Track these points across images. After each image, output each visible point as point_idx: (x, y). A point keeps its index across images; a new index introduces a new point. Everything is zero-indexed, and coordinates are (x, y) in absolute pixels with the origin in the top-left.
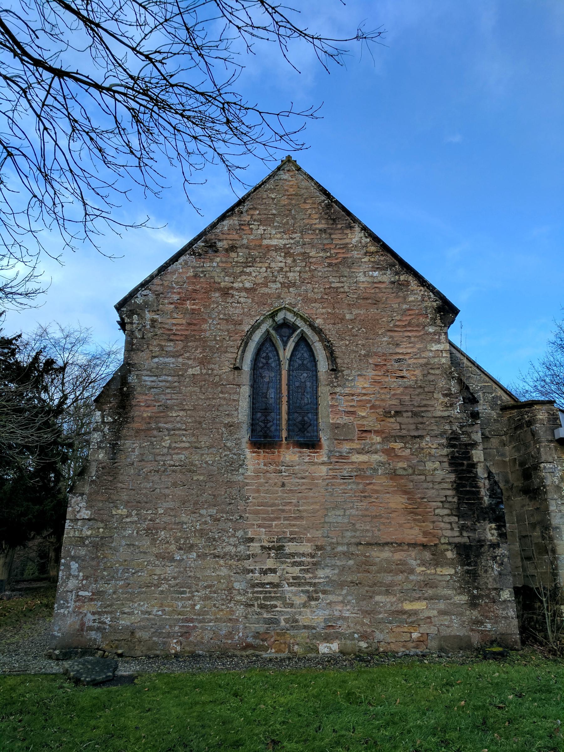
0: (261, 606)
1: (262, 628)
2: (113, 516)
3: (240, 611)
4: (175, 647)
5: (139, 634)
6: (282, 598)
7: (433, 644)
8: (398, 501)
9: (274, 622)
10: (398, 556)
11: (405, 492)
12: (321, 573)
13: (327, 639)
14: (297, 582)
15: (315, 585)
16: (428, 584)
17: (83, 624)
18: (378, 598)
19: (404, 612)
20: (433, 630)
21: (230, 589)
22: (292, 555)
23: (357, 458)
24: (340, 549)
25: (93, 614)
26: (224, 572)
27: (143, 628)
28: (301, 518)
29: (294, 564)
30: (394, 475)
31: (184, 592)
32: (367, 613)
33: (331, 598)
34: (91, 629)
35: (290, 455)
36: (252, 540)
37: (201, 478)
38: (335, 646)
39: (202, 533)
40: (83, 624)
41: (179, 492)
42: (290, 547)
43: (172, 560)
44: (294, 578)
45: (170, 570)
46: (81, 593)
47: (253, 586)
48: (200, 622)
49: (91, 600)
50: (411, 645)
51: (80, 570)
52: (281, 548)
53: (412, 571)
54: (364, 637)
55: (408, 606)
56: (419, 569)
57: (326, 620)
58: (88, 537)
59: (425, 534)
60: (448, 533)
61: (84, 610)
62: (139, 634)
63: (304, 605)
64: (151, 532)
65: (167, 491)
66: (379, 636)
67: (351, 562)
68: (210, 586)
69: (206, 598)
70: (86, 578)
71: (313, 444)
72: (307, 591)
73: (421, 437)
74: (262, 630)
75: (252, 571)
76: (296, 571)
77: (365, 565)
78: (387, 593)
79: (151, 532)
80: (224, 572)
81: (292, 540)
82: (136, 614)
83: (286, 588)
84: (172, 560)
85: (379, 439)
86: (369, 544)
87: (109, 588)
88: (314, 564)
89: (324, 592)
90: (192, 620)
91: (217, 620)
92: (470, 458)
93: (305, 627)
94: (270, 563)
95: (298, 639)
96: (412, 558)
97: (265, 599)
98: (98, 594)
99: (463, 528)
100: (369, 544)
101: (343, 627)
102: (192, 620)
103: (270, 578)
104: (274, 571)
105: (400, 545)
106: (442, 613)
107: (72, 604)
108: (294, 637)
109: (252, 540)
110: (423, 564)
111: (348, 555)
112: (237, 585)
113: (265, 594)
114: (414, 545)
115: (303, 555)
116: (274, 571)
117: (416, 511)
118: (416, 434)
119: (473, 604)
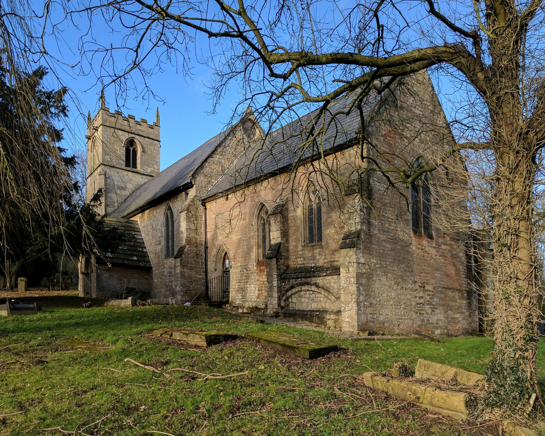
1: (419, 323)
3: (414, 315)
6: (425, 310)
9: (423, 321)
10: (453, 294)
12: (435, 299)
13: (437, 329)
14: (429, 303)
15: (433, 305)
16: (460, 307)
17: (367, 319)
18: (449, 312)
19: (454, 318)
20: (461, 326)
22: (428, 290)
23: (444, 247)
24: (440, 289)
25: (370, 314)
28: (428, 273)
29: (429, 295)
31: (397, 305)
32: (447, 318)
33: (438, 311)
35: (425, 242)
36: (416, 282)
37: (399, 247)
40: (367, 319)
42: (428, 287)
44: (428, 301)
46: (365, 303)
47: (417, 304)
50: (456, 332)
51: (364, 290)
52: (424, 287)
53: (456, 302)
54: (446, 328)
56: (459, 300)
57: (437, 321)
58: (365, 273)
59: (460, 285)
60: (465, 286)
65: (389, 252)
66: (449, 328)
67: (442, 296)
70: (366, 295)
71: (431, 237)
72: (431, 308)
73: (458, 240)
74: (420, 324)
75: (416, 297)
77: (446, 296)
78: (451, 310)
80: (409, 297)
81: (427, 283)
86: (447, 288)
89: (436, 309)
90: (401, 319)
94: (421, 294)
95: (430, 329)
96: (457, 295)
97: (422, 310)
101: (441, 324)
102: (401, 319)
103: (422, 301)
105: (454, 289)
106: (464, 319)
108: (429, 327)
109: (416, 282)
110: (459, 299)
111: (441, 292)
114: (457, 290)
115: (430, 291)
118: (457, 238)
119: (470, 316)
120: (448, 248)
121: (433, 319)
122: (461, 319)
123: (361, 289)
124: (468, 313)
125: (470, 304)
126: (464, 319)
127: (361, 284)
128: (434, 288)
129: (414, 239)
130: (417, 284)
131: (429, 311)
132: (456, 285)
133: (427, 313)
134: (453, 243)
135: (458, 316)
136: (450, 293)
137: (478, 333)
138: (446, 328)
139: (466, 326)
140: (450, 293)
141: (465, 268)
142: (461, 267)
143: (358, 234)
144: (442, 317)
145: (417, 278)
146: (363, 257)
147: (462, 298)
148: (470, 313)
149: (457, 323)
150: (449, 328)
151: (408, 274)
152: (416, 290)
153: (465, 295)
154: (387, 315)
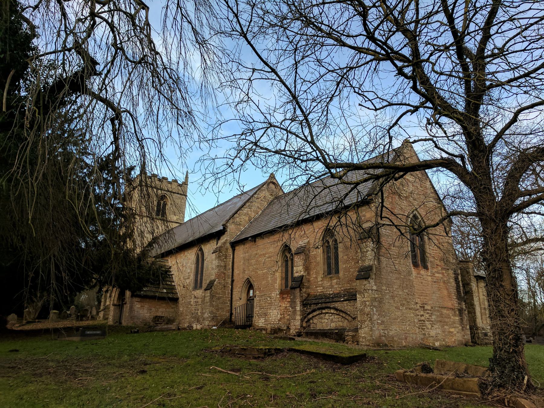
0: (422, 329)
1: (422, 336)
2: (382, 289)
4: (404, 344)
5: (395, 338)
6: (426, 326)
7: (457, 343)
8: (445, 292)
9: (424, 334)
10: (448, 312)
11: (447, 289)
12: (434, 317)
14: (429, 320)
15: (432, 321)
17: (380, 334)
18: (445, 327)
19: (450, 332)
21: (414, 322)
22: (427, 310)
23: (437, 275)
24: (437, 308)
26: (412, 315)
27: (395, 336)
28: (427, 296)
29: (428, 313)
30: (444, 282)
32: (444, 332)
33: (436, 326)
34: (383, 336)
35: (423, 272)
36: (417, 303)
38: (438, 343)
39: (405, 299)
40: (380, 334)
41: (398, 282)
42: (426, 307)
43: (400, 310)
45: (399, 314)
48: (409, 334)
49: (381, 324)
51: (377, 311)
52: (424, 307)
55: (452, 330)
56: (452, 317)
59: (452, 305)
60: (457, 305)
61: (380, 328)
62: (395, 339)
63: (431, 329)
64: (393, 297)
65: (395, 281)
68: (409, 320)
69: (409, 325)
70: (379, 315)
71: (426, 267)
76: (427, 315)
77: (442, 314)
78: (447, 325)
79: (393, 297)
81: (426, 304)
82: (394, 330)
83: (426, 322)
84: (400, 310)
85: (440, 269)
86: (442, 307)
87: (385, 319)
88: (432, 314)
91: (412, 333)
92: (458, 279)
93: (432, 337)
94: (422, 313)
96: (450, 313)
97: (423, 326)
98: (383, 322)
99: (459, 304)
100: (442, 307)
103: (423, 318)
104: (423, 315)
106: (458, 332)
107: (376, 326)
111: (438, 311)
112: (416, 320)
113: (422, 325)
114: (450, 309)
116: (423, 315)
117: (449, 296)
119: (463, 330)
120: (440, 275)
121: (433, 333)
122: (455, 332)
123: (375, 310)
124: (460, 328)
125: (462, 319)
126: (458, 332)
127: (374, 306)
128: (432, 308)
129: (413, 270)
130: (418, 305)
131: (430, 327)
132: (449, 305)
133: (428, 329)
134: (444, 272)
135: (452, 330)
136: (445, 311)
137: (471, 344)
138: (444, 340)
139: (460, 339)
140: (445, 311)
141: (455, 291)
142: (452, 290)
143: (369, 269)
144: (439, 331)
145: (418, 300)
146: (376, 285)
147: (455, 315)
148: (463, 327)
149: (452, 336)
150: (447, 340)
151: (411, 297)
152: (418, 309)
153: (457, 313)
154: (396, 330)
